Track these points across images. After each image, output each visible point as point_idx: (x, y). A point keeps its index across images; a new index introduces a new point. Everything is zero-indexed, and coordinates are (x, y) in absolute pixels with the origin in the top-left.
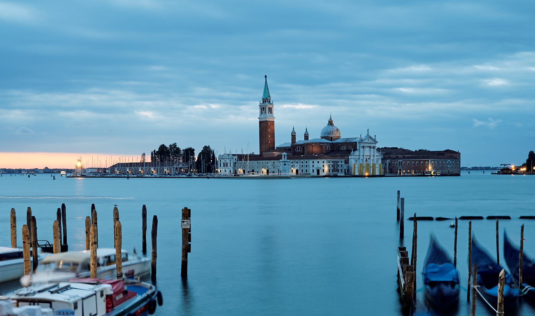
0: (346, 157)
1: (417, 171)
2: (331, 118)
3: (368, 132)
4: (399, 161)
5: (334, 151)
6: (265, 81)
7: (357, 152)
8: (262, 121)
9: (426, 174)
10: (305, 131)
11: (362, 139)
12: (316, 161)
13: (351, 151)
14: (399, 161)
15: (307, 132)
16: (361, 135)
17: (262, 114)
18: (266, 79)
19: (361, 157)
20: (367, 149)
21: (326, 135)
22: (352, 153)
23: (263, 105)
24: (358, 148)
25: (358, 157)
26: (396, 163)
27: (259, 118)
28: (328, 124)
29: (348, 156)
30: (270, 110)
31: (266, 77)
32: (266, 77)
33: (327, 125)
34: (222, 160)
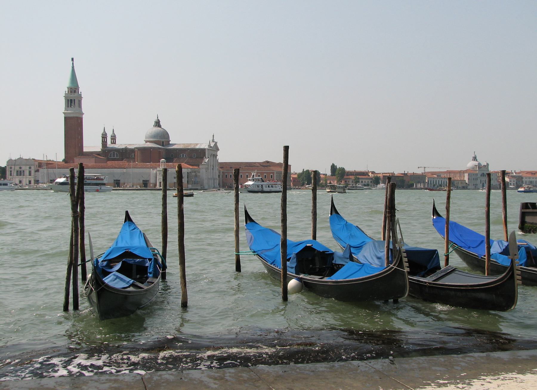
6: (72, 66)
8: (69, 117)
15: (114, 134)
18: (73, 63)
25: (207, 166)
26: (231, 175)
29: (198, 165)
31: (73, 59)
32: (73, 59)
34: (13, 167)
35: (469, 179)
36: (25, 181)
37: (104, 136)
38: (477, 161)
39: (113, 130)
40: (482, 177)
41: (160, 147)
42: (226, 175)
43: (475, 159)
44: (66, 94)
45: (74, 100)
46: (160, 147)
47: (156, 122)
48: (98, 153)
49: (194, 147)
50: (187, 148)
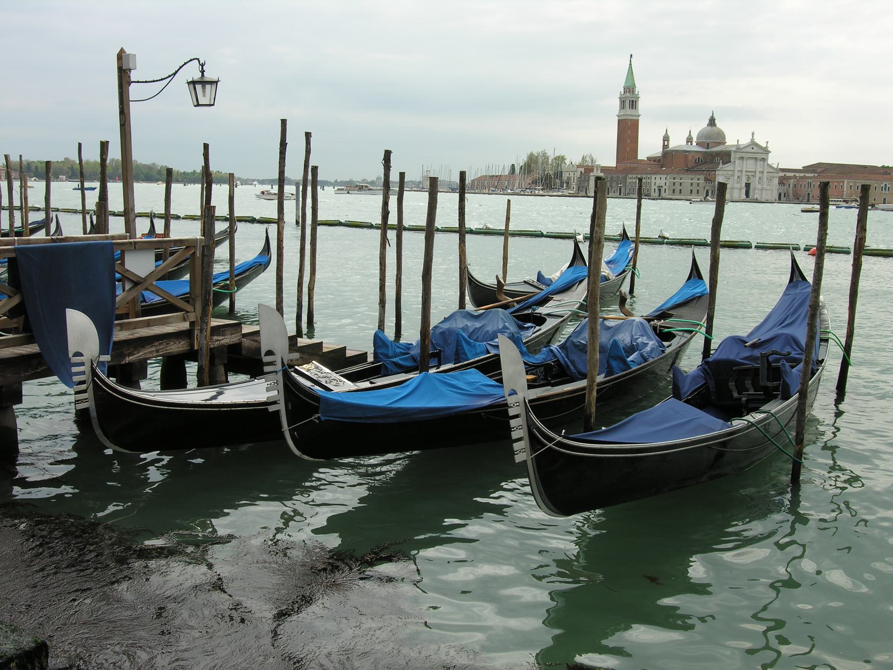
0: (713, 173)
2: (714, 115)
3: (753, 137)
5: (707, 163)
7: (730, 166)
10: (689, 134)
11: (738, 147)
12: (658, 177)
13: (719, 164)
16: (738, 141)
19: (737, 174)
20: (751, 162)
22: (720, 167)
23: (624, 96)
24: (732, 160)
25: (731, 173)
28: (708, 125)
30: (633, 104)
32: (631, 56)
33: (706, 126)
37: (666, 139)
39: (690, 131)
44: (621, 94)
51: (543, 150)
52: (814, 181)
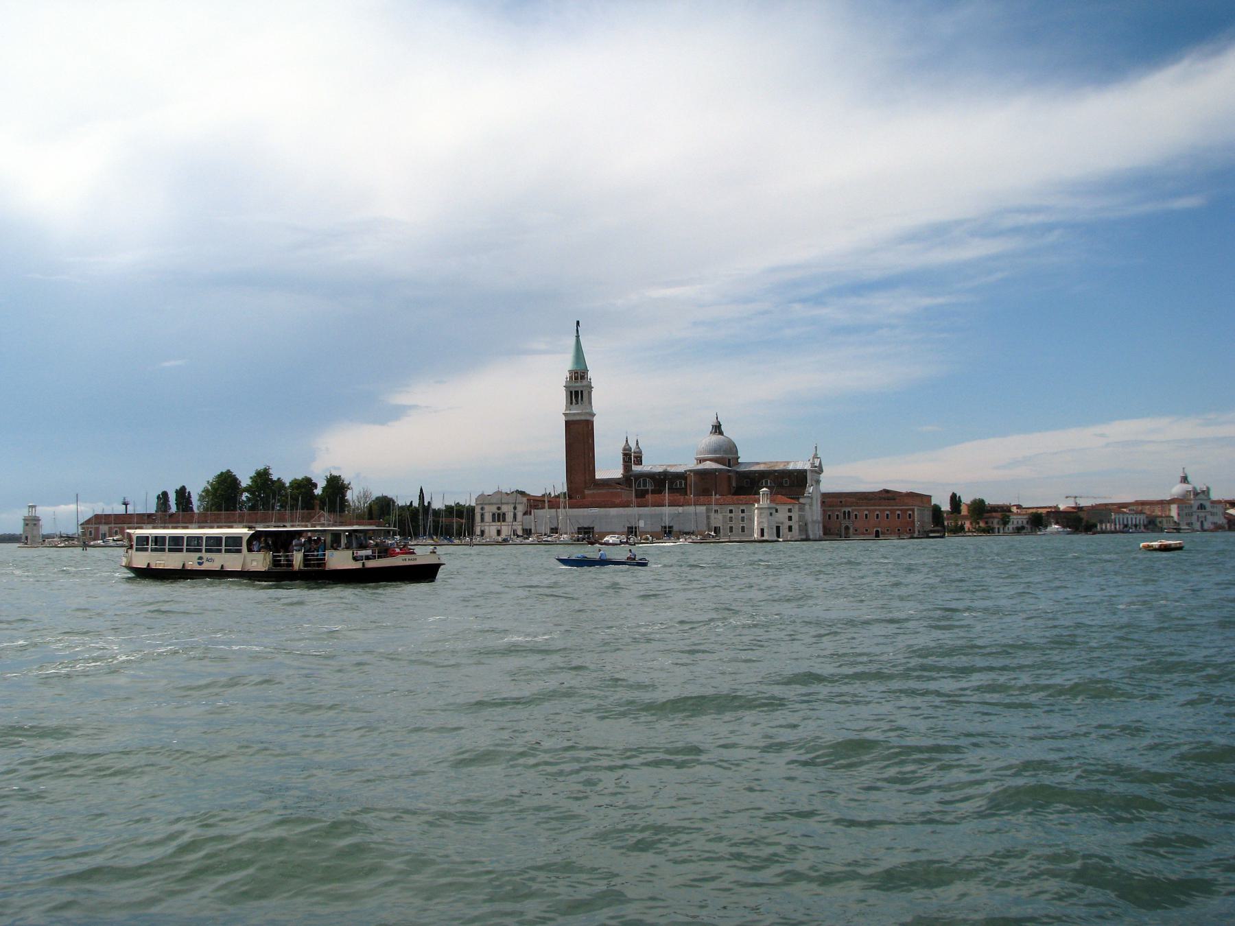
1: (888, 530)
3: (816, 450)
4: (845, 512)
8: (573, 421)
9: (931, 535)
14: (845, 512)
15: (639, 448)
17: (571, 403)
21: (718, 456)
23: (577, 384)
26: (837, 515)
27: (565, 415)
29: (799, 498)
31: (578, 323)
32: (578, 323)
34: (487, 508)
35: (1179, 515)
36: (506, 531)
38: (1188, 483)
39: (637, 441)
40: (1200, 510)
41: (724, 467)
42: (829, 516)
43: (1185, 480)
45: (582, 391)
46: (724, 467)
47: (716, 426)
48: (616, 482)
49: (784, 468)
50: (773, 469)
51: (263, 467)
52: (856, 510)
